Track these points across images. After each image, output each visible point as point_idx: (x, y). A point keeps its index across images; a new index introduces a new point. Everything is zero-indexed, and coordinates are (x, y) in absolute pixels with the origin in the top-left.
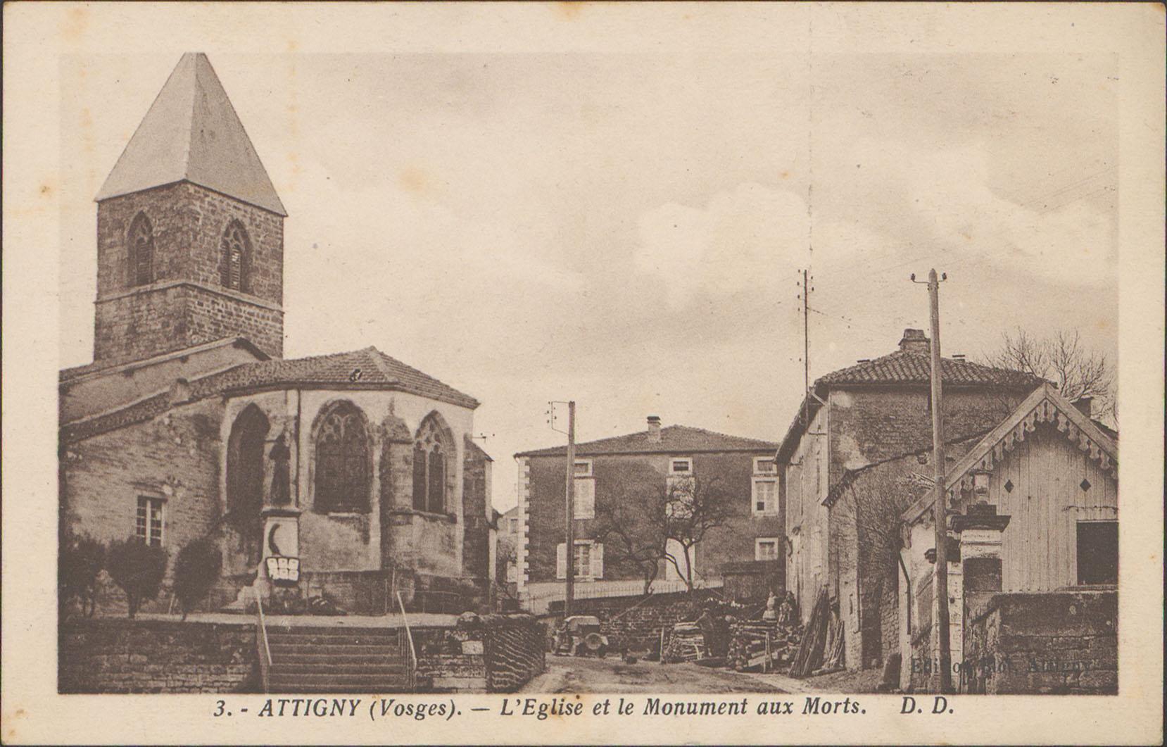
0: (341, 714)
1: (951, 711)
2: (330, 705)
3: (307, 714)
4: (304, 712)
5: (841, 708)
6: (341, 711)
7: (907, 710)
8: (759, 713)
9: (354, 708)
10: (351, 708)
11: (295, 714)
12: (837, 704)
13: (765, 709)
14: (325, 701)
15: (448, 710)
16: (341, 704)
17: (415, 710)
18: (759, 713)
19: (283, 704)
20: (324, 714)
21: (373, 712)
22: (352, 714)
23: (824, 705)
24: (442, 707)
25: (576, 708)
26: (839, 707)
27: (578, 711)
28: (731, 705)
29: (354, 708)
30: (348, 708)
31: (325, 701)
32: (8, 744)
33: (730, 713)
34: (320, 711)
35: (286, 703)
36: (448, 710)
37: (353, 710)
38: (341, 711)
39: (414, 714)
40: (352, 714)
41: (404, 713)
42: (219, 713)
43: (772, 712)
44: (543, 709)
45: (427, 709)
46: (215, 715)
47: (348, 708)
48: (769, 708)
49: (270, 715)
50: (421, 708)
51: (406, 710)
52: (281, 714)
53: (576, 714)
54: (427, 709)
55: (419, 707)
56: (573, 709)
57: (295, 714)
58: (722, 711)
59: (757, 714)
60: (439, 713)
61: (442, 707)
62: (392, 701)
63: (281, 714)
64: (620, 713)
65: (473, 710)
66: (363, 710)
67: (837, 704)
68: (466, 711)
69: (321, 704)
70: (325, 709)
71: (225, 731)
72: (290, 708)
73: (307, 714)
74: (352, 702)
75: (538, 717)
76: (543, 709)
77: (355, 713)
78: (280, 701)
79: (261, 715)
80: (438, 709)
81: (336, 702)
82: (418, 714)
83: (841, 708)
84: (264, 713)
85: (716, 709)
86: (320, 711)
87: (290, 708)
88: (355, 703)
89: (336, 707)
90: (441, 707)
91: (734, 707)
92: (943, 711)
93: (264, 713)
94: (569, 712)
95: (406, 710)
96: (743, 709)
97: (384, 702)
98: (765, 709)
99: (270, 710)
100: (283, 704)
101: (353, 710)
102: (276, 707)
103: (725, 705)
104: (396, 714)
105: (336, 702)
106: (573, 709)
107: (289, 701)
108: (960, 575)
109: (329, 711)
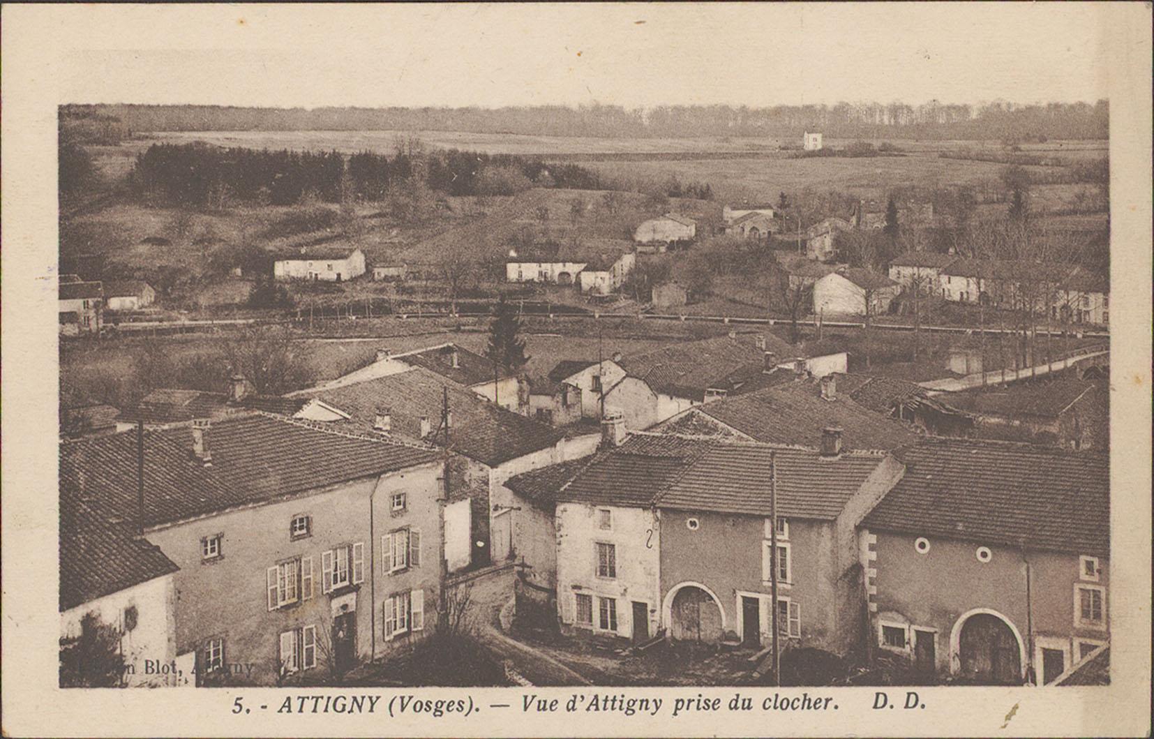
0: (360, 711)
1: (892, 707)
2: (349, 702)
3: (326, 711)
4: (298, 709)
5: (694, 704)
6: (360, 708)
7: (878, 706)
8: (731, 709)
9: (373, 704)
10: (369, 704)
11: (315, 711)
12: (690, 701)
13: (736, 705)
14: (345, 698)
15: (466, 706)
16: (360, 700)
17: (433, 706)
18: (569, 710)
19: (317, 701)
20: (343, 710)
21: (393, 708)
22: (371, 710)
23: (783, 700)
24: (461, 703)
25: (714, 704)
26: (692, 704)
27: (716, 707)
28: (642, 701)
29: (373, 704)
30: (367, 704)
31: (345, 698)
32: (12, 736)
33: (803, 708)
34: (339, 707)
35: (306, 700)
36: (466, 706)
37: (372, 707)
38: (360, 708)
39: (433, 710)
40: (371, 710)
41: (423, 710)
42: (237, 710)
43: (775, 708)
44: (631, 704)
45: (445, 705)
46: (234, 711)
47: (367, 704)
48: (740, 704)
49: (289, 711)
50: (439, 704)
51: (424, 706)
52: (301, 711)
53: (714, 709)
54: (445, 705)
55: (437, 704)
56: (710, 704)
57: (315, 711)
58: (817, 706)
59: (566, 711)
60: (457, 709)
61: (461, 703)
62: (411, 698)
63: (301, 711)
64: (539, 710)
65: (492, 706)
66: (382, 706)
67: (690, 701)
68: (255, 708)
69: (341, 701)
70: (344, 705)
71: (241, 725)
72: (309, 704)
73: (326, 711)
74: (370, 698)
75: (434, 714)
76: (631, 704)
77: (374, 709)
78: (299, 698)
79: (280, 711)
80: (456, 705)
81: (355, 698)
82: (436, 710)
83: (694, 704)
84: (283, 709)
85: (812, 705)
86: (339, 707)
87: (309, 704)
88: (374, 699)
89: (355, 703)
90: (708, 706)
91: (645, 703)
92: (883, 706)
93: (283, 709)
94: (706, 707)
95: (424, 706)
96: (613, 706)
97: (402, 698)
98: (736, 705)
99: (289, 707)
100: (317, 701)
101: (372, 707)
102: (295, 704)
103: (821, 700)
104: (415, 710)
105: (355, 698)
106: (710, 704)
107: (308, 698)
108: (949, 278)
109: (348, 708)
